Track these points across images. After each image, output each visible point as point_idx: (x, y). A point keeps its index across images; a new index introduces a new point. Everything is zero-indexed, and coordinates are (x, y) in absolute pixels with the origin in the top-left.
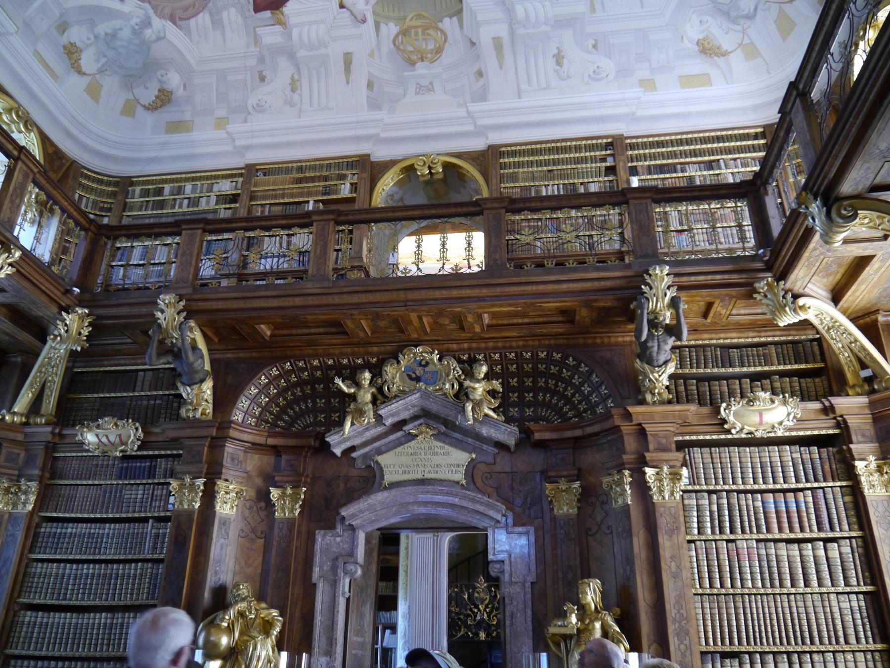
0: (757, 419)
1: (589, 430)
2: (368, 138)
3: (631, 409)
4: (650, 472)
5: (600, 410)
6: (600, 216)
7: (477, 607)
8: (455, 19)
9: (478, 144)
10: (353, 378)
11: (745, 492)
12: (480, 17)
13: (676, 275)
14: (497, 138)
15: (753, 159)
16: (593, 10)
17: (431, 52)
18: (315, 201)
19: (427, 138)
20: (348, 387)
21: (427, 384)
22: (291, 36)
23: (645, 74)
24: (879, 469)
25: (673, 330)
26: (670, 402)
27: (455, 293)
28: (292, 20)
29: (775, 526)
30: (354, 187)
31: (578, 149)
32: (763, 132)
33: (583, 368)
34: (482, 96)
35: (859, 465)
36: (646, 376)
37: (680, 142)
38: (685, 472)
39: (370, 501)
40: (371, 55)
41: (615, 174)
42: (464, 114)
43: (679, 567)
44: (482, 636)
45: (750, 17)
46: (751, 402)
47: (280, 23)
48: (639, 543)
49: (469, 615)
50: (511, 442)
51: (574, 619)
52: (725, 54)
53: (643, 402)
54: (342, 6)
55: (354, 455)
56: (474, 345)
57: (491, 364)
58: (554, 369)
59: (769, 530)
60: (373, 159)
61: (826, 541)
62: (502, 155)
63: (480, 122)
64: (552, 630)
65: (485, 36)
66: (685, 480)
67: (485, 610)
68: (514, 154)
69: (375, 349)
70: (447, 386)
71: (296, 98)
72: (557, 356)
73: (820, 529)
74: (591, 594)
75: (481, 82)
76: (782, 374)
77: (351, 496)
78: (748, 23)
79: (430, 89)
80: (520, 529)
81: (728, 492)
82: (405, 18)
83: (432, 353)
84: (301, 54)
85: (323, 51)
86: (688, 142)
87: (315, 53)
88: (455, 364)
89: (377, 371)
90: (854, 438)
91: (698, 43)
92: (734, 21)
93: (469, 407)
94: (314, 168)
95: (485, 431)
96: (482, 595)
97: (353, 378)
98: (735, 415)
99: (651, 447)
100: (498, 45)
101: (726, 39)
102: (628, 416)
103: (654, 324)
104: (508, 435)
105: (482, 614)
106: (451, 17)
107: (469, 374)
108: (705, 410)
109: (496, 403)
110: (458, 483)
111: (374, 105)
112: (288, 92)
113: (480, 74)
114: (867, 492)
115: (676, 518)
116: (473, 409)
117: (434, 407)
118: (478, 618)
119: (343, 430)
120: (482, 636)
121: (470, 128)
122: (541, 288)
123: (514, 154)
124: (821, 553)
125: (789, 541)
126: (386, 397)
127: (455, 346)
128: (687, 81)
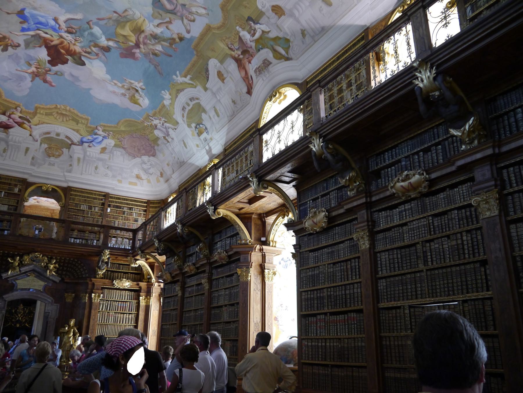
0: (121, 284)
1: (80, 281)
2: (28, 174)
3: (92, 279)
4: (93, 295)
5: (84, 276)
6: (97, 218)
7: (18, 315)
8: (67, 149)
9: (65, 185)
10: (13, 258)
11: (115, 301)
12: (75, 151)
13: (110, 252)
14: (71, 185)
15: (142, 209)
16: (110, 159)
17: (57, 155)
18: (5, 192)
19: (48, 179)
20: (11, 260)
21: (37, 262)
22: (8, 137)
23: (120, 179)
24: (145, 299)
25: (107, 263)
26: (102, 278)
27: (53, 247)
28: (11, 133)
29: (119, 310)
30: (20, 190)
31: (95, 194)
32: (147, 202)
33: (82, 265)
34: (70, 171)
35: (141, 298)
36: (98, 271)
37: (124, 199)
38: (102, 295)
39: (13, 294)
40: (36, 150)
41: (104, 206)
42: (62, 174)
43: (95, 318)
44: (18, 325)
45: (151, 174)
46: (121, 280)
47: (6, 133)
48: (86, 312)
49: (13, 318)
50: (58, 281)
51: (67, 328)
52: (142, 180)
53: (95, 277)
54: (30, 135)
55: (8, 279)
56: (53, 254)
57: (56, 259)
58: (74, 263)
59: (118, 310)
60: (28, 181)
61: (130, 314)
62: (72, 190)
63: (67, 178)
64: (61, 331)
65: (76, 156)
66: (101, 297)
67: (21, 316)
68: (75, 191)
69: (22, 251)
70: (43, 264)
71: (4, 154)
72: (76, 260)
73: (129, 311)
74: (72, 323)
75: (71, 168)
76: (131, 273)
77: (6, 292)
78: (150, 175)
79: (54, 165)
80: (56, 304)
81: (111, 301)
82: (51, 144)
83: (40, 255)
84: (10, 143)
85: (19, 144)
86: (127, 200)
87: (16, 144)
88: (46, 259)
89: (21, 257)
90: (142, 291)
91: (136, 175)
92: (147, 173)
93: (48, 272)
94: (6, 179)
95: (51, 278)
96: (20, 311)
97: (14, 259)
98: (117, 283)
99: (95, 288)
100: (79, 159)
101: (144, 176)
102: (91, 281)
103: (103, 261)
104: (57, 279)
105: (19, 317)
106: (66, 148)
107: (50, 261)
108: (110, 281)
109: (55, 270)
110: (40, 290)
111: (32, 164)
112: (2, 152)
113: (71, 165)
114: (141, 304)
115: (97, 306)
116: (49, 272)
117: (36, 269)
118: (17, 319)
119: (8, 273)
120: (18, 325)
121: (63, 179)
122: (77, 249)
123: (75, 191)
124: (128, 316)
125: (121, 313)
126: (22, 264)
127: (47, 254)
128: (131, 183)
